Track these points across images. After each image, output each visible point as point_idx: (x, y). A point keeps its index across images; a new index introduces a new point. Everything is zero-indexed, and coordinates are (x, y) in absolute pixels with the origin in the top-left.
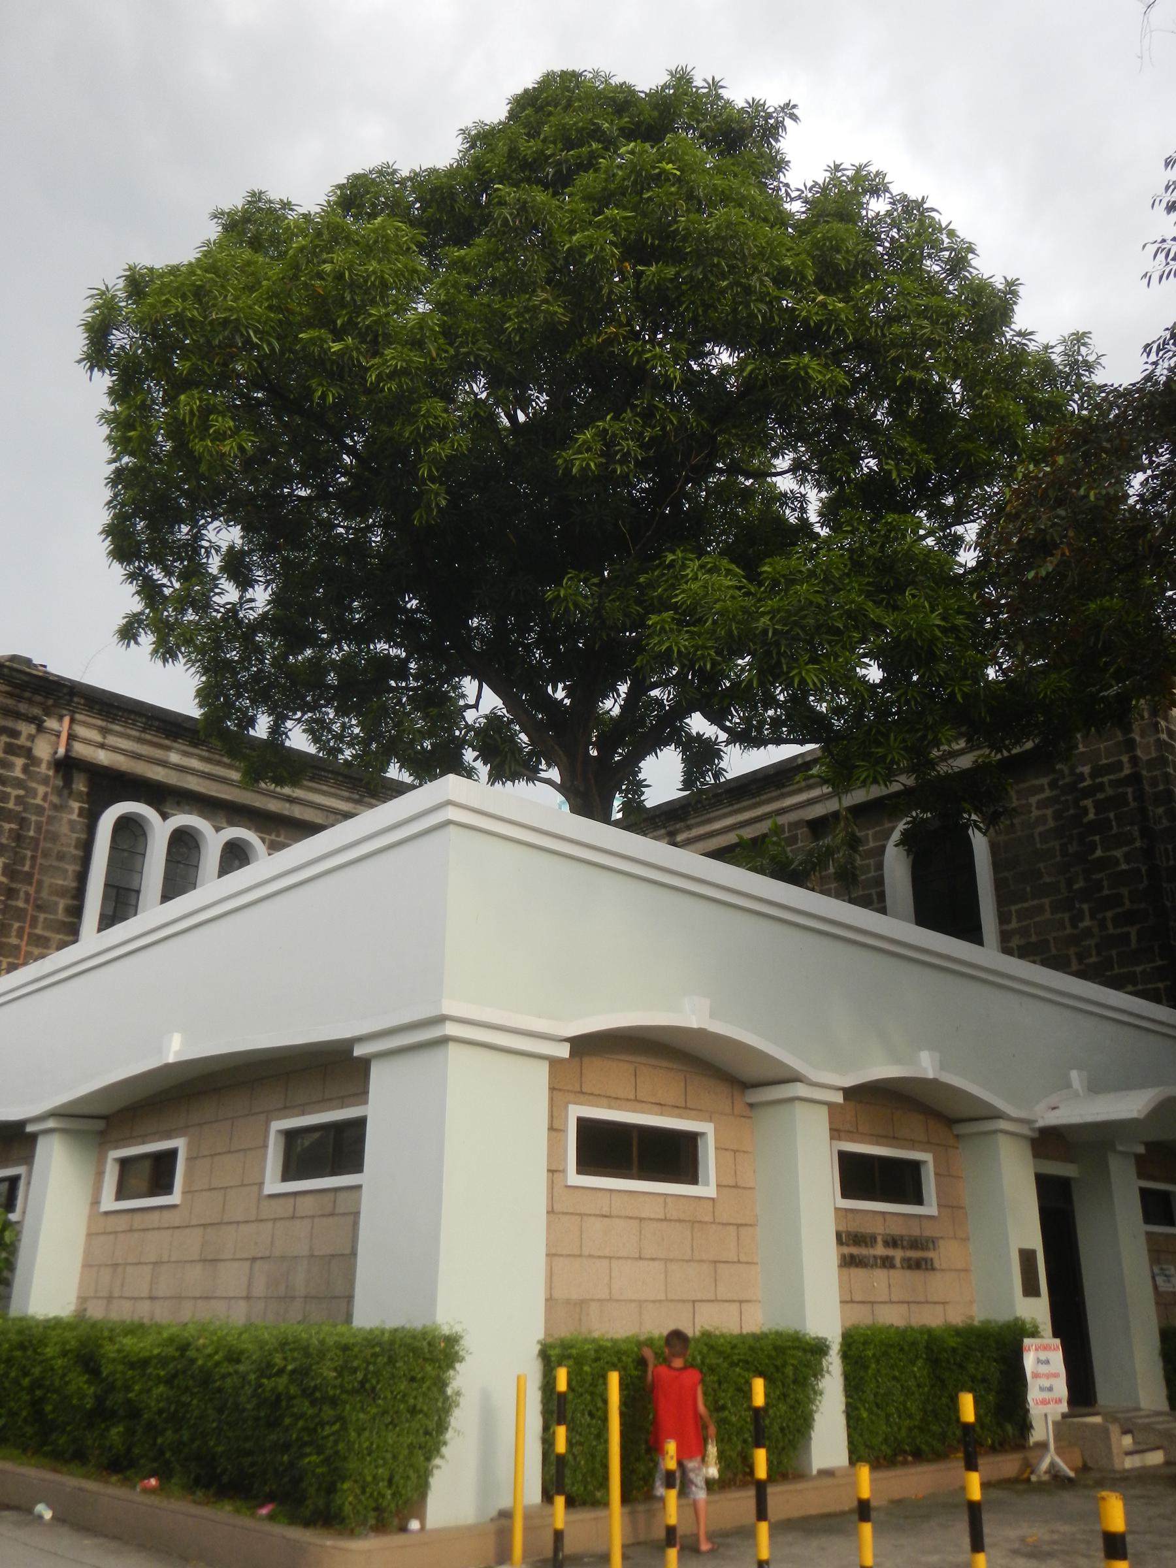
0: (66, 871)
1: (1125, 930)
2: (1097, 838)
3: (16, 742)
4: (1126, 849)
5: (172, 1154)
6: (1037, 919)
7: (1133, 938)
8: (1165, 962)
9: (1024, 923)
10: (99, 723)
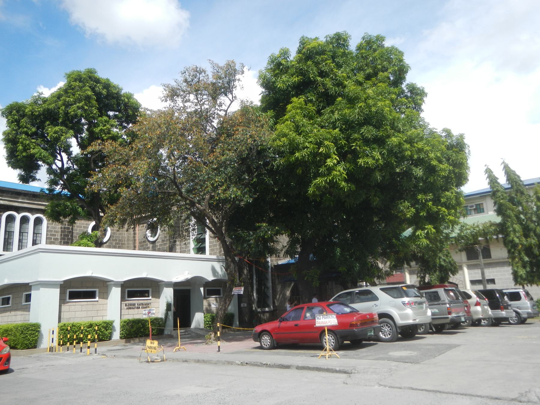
5: (10, 297)
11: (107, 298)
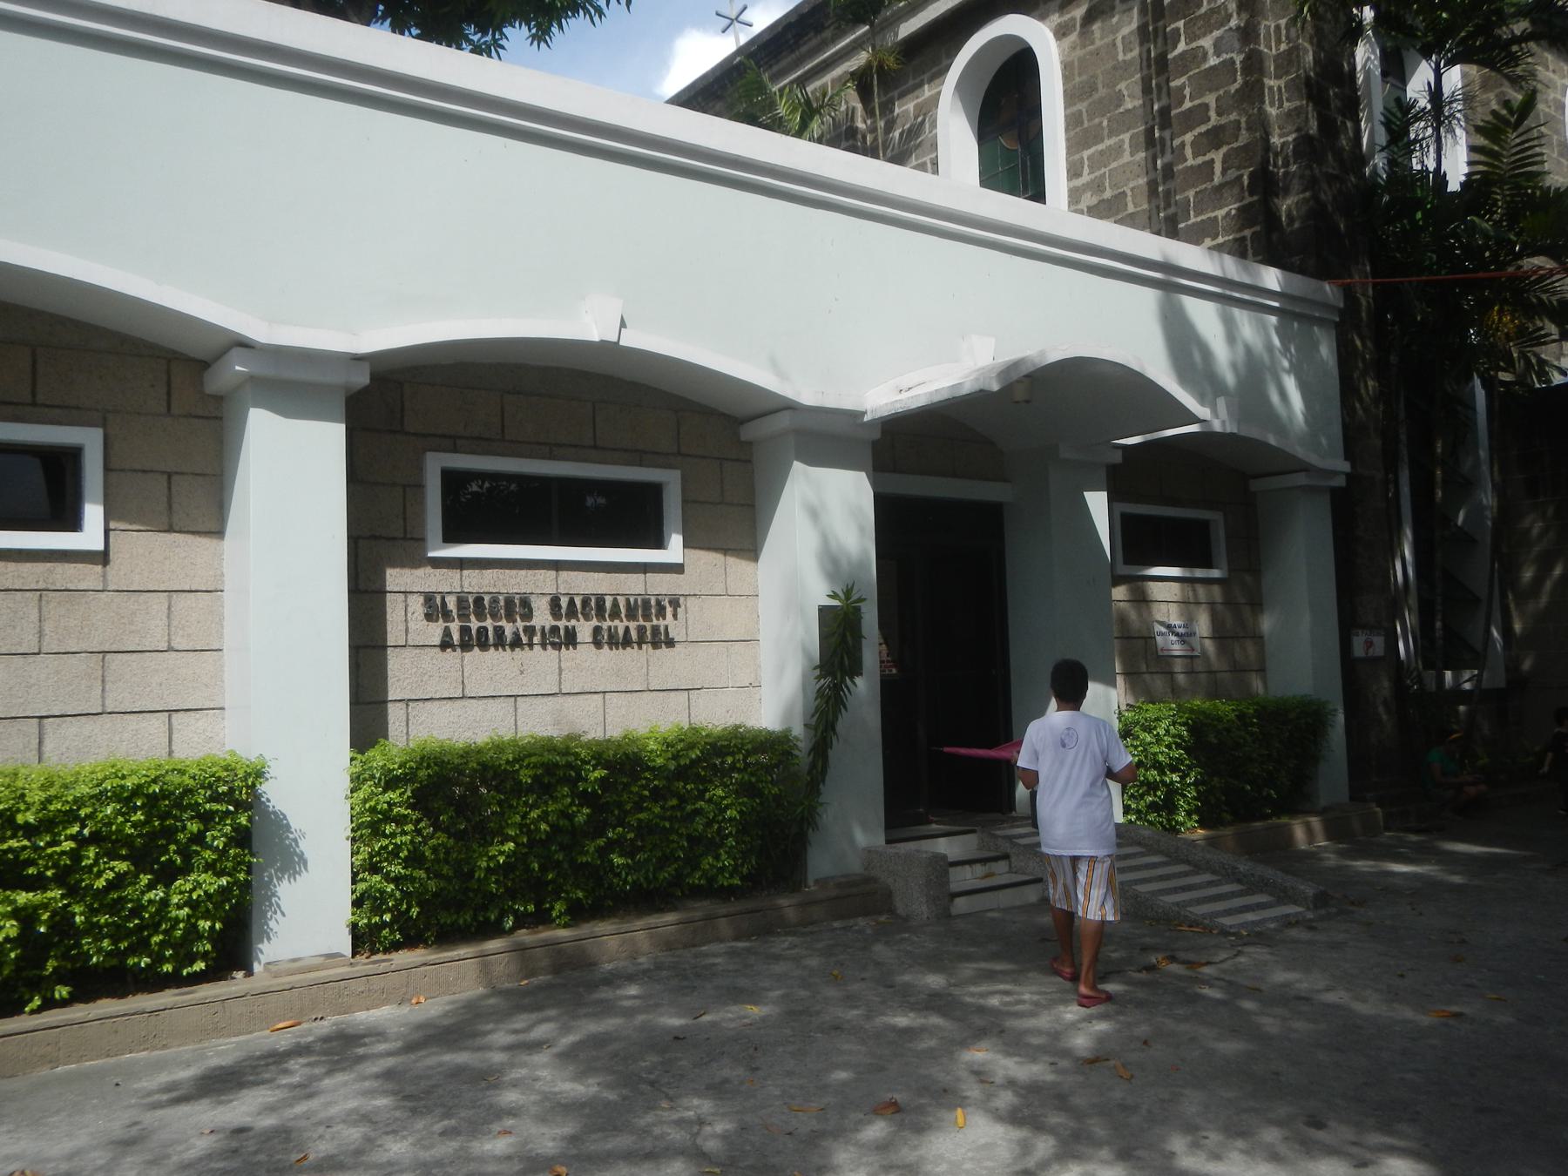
1: (1208, 157)
2: (1181, 24)
4: (1217, 33)
6: (1114, 165)
7: (1218, 167)
8: (1255, 198)
9: (1097, 174)
11: (217, 531)
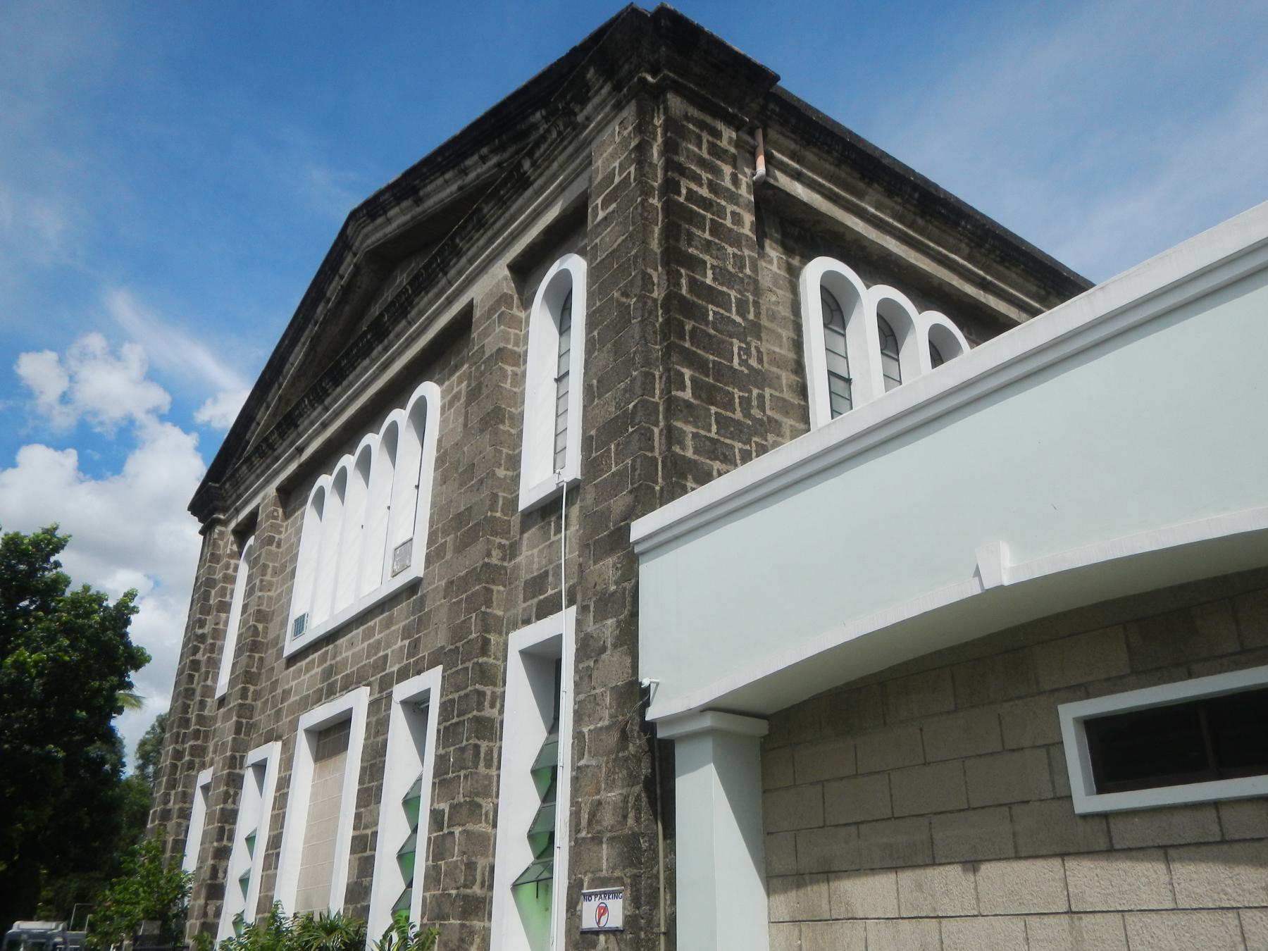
0: (780, 336)
3: (719, 143)
10: (792, 146)
